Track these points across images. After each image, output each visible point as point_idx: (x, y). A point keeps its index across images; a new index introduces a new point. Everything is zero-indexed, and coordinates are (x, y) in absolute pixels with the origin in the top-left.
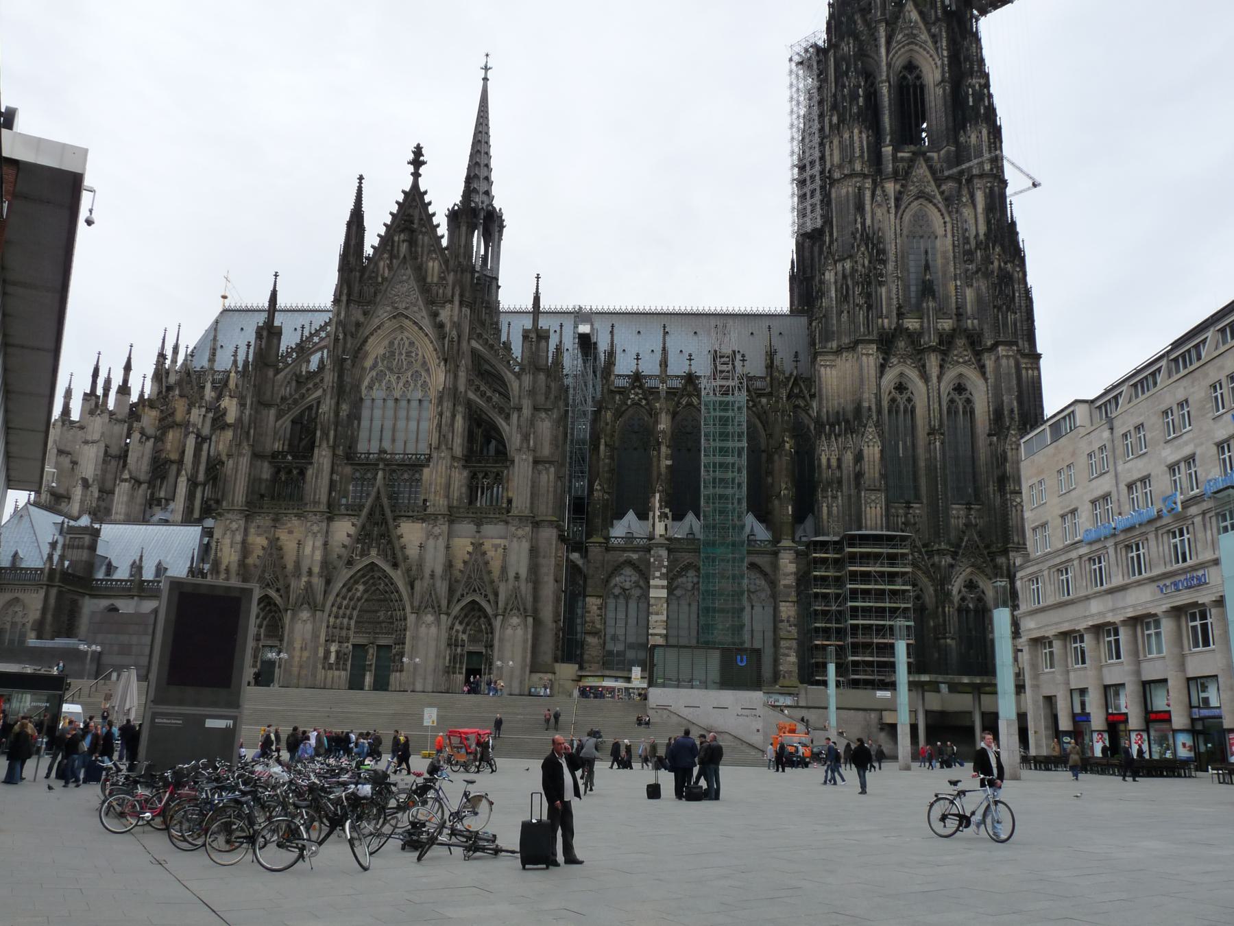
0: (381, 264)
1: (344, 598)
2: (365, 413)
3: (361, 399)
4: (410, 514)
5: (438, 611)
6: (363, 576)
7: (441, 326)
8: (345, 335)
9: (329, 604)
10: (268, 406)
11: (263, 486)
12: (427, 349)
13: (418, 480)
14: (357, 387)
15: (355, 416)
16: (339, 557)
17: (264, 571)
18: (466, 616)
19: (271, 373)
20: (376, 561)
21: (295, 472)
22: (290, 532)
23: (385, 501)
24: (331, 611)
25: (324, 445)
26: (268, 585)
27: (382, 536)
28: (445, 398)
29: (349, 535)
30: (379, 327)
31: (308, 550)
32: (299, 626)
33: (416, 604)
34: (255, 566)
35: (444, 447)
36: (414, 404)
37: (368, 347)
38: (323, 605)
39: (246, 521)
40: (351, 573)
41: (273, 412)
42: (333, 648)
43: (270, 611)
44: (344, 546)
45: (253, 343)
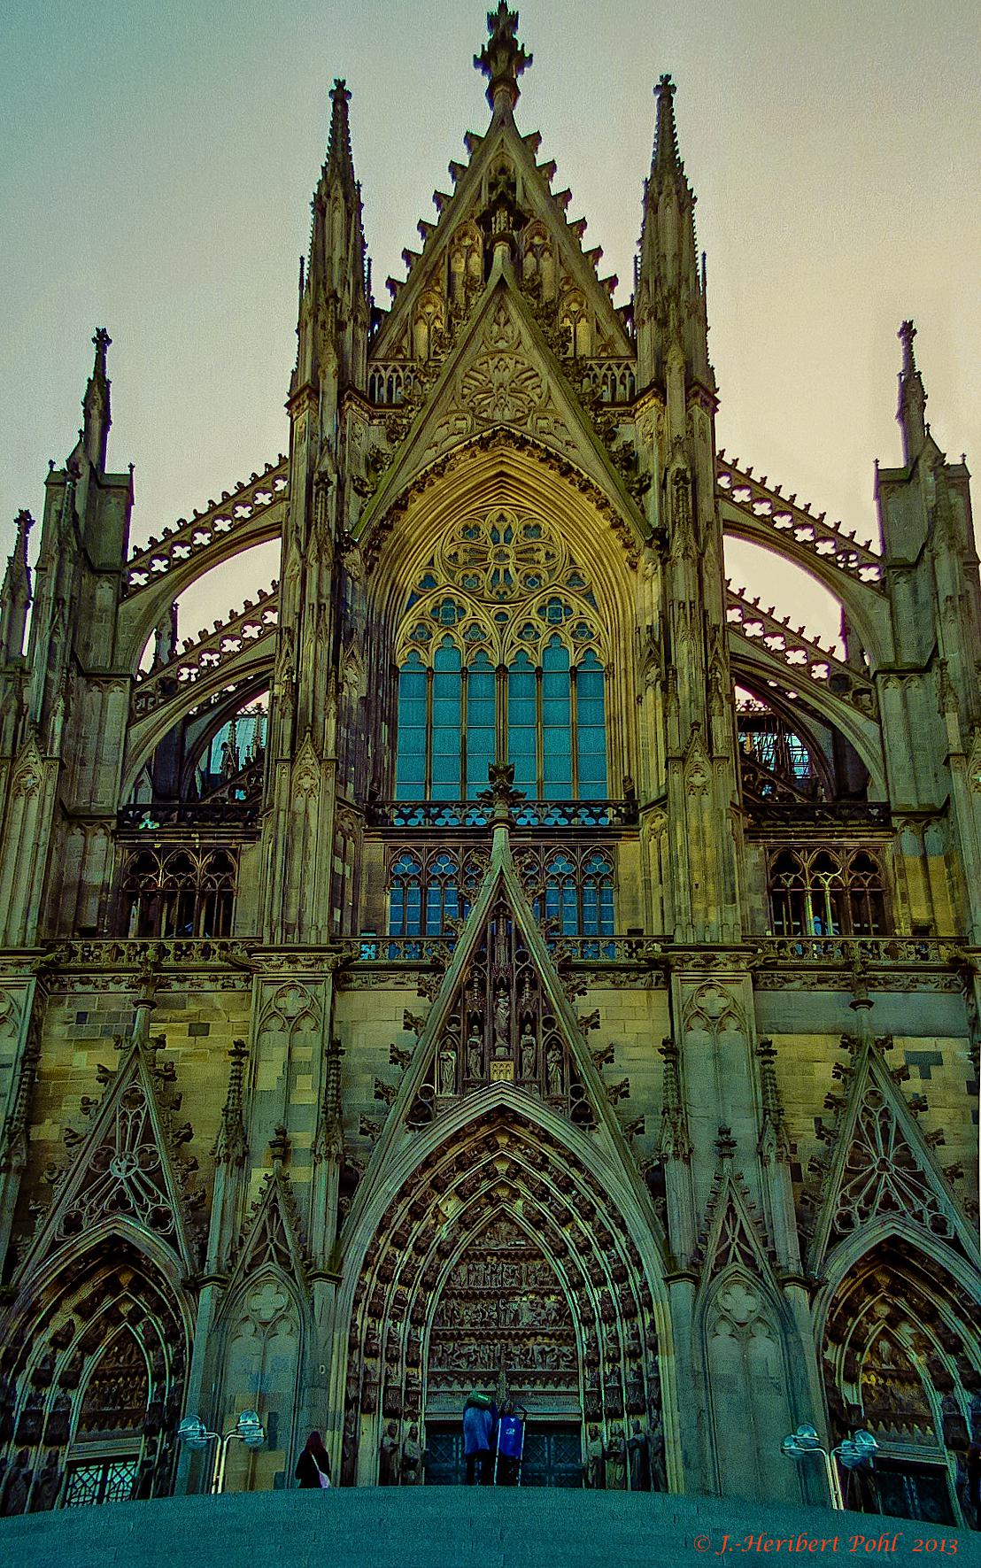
0: (422, 331)
1: (399, 1243)
2: (408, 709)
3: (394, 668)
4: (604, 960)
5: (766, 1273)
6: (462, 1163)
7: (628, 460)
8: (341, 487)
9: (354, 1257)
10: (101, 678)
11: (92, 906)
12: (583, 530)
13: (610, 877)
14: (381, 632)
15: (379, 710)
16: (383, 1093)
17: (104, 1159)
18: (851, 1309)
19: (105, 593)
20: (515, 1102)
21: (200, 864)
22: (199, 1029)
23: (524, 916)
24: (362, 1287)
25: (308, 757)
26: (120, 1203)
27: (526, 1021)
28: (681, 627)
29: (410, 1023)
30: (439, 470)
31: (269, 1076)
32: (244, 1347)
33: (682, 1245)
34: (73, 1138)
35: (698, 757)
36: (556, 683)
37: (408, 524)
38: (337, 1260)
39: (39, 995)
40: (430, 1143)
41: (117, 697)
42: (370, 1432)
43: (112, 1317)
44: (398, 1057)
45: (38, 516)
